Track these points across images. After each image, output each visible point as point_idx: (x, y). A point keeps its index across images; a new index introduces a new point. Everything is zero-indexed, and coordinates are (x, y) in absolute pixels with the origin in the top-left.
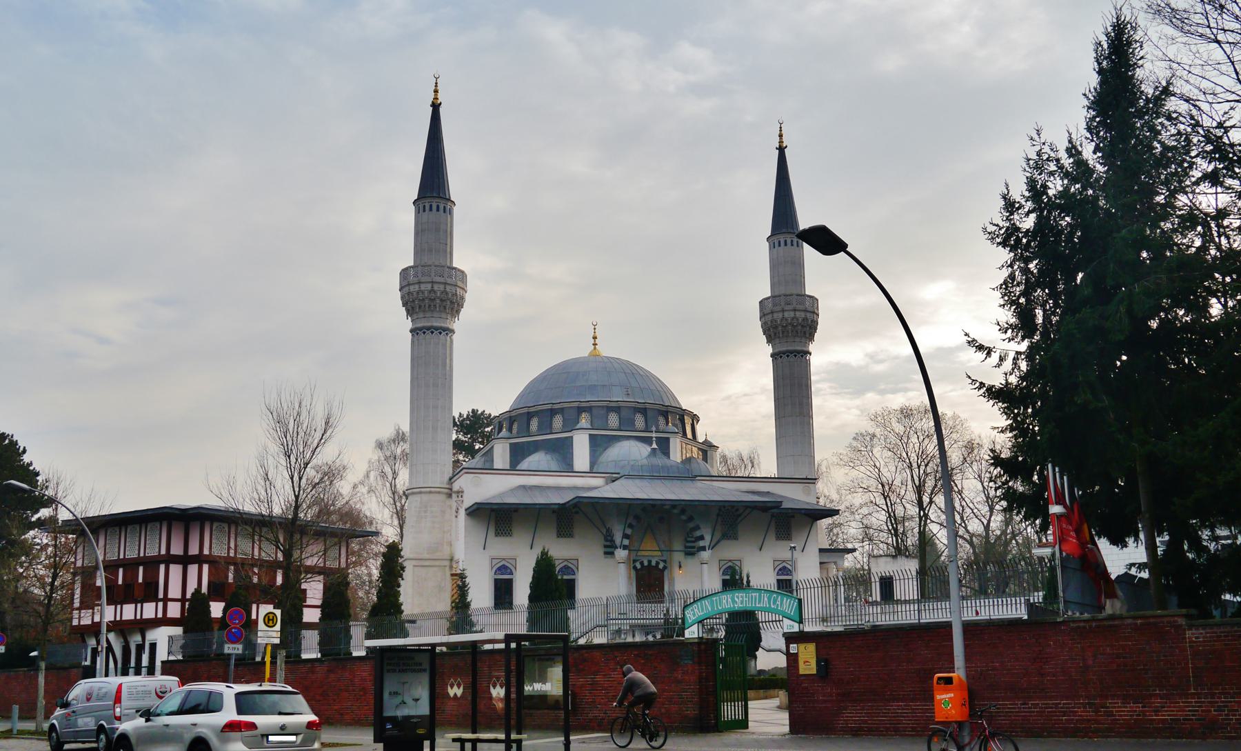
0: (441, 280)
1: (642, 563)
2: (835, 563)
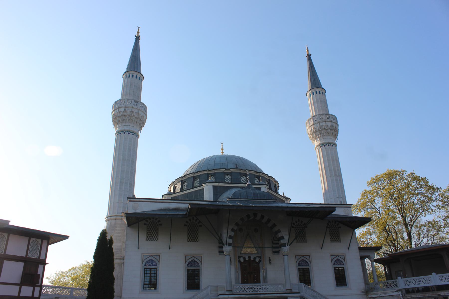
0: (130, 106)
1: (244, 258)
2: (368, 257)
